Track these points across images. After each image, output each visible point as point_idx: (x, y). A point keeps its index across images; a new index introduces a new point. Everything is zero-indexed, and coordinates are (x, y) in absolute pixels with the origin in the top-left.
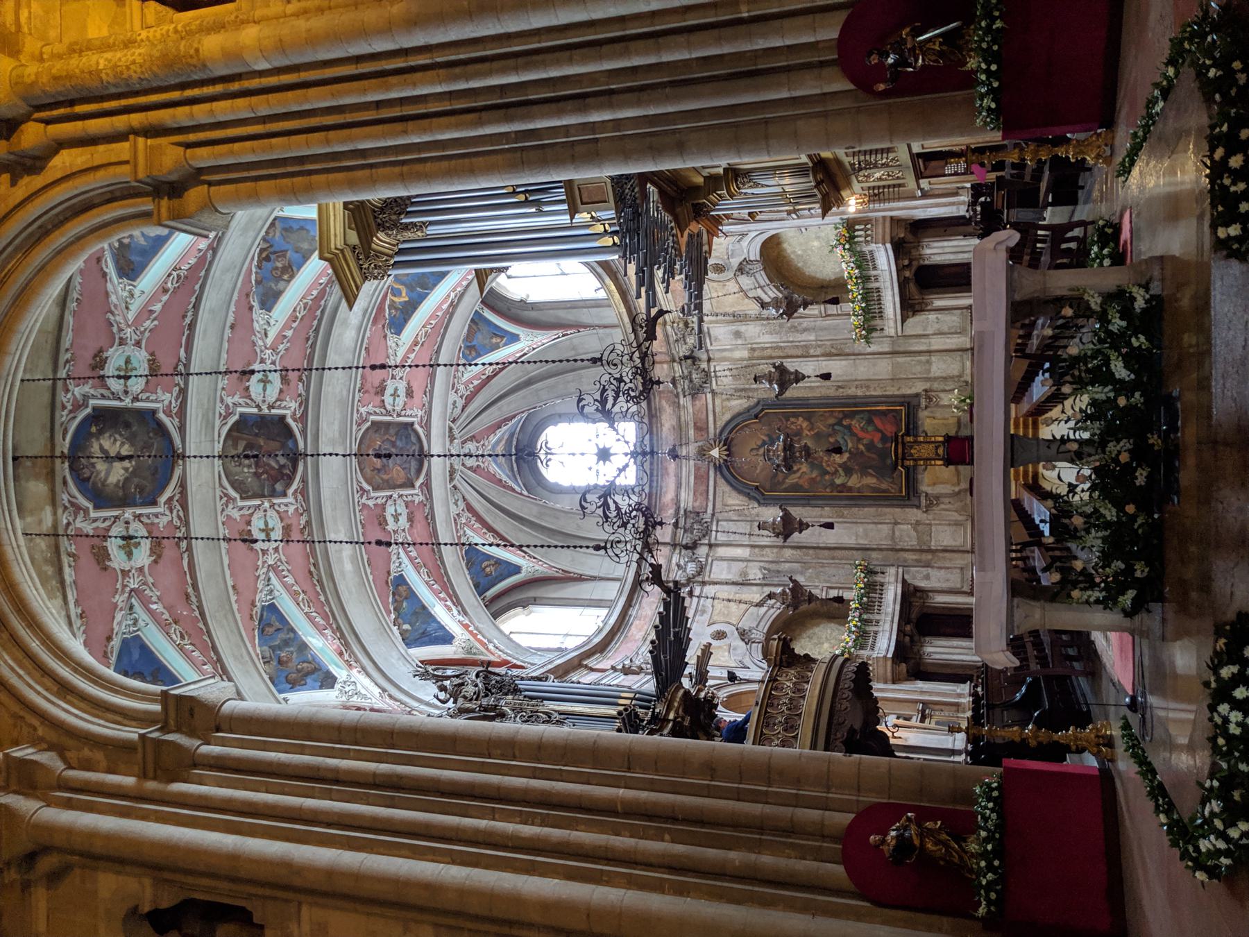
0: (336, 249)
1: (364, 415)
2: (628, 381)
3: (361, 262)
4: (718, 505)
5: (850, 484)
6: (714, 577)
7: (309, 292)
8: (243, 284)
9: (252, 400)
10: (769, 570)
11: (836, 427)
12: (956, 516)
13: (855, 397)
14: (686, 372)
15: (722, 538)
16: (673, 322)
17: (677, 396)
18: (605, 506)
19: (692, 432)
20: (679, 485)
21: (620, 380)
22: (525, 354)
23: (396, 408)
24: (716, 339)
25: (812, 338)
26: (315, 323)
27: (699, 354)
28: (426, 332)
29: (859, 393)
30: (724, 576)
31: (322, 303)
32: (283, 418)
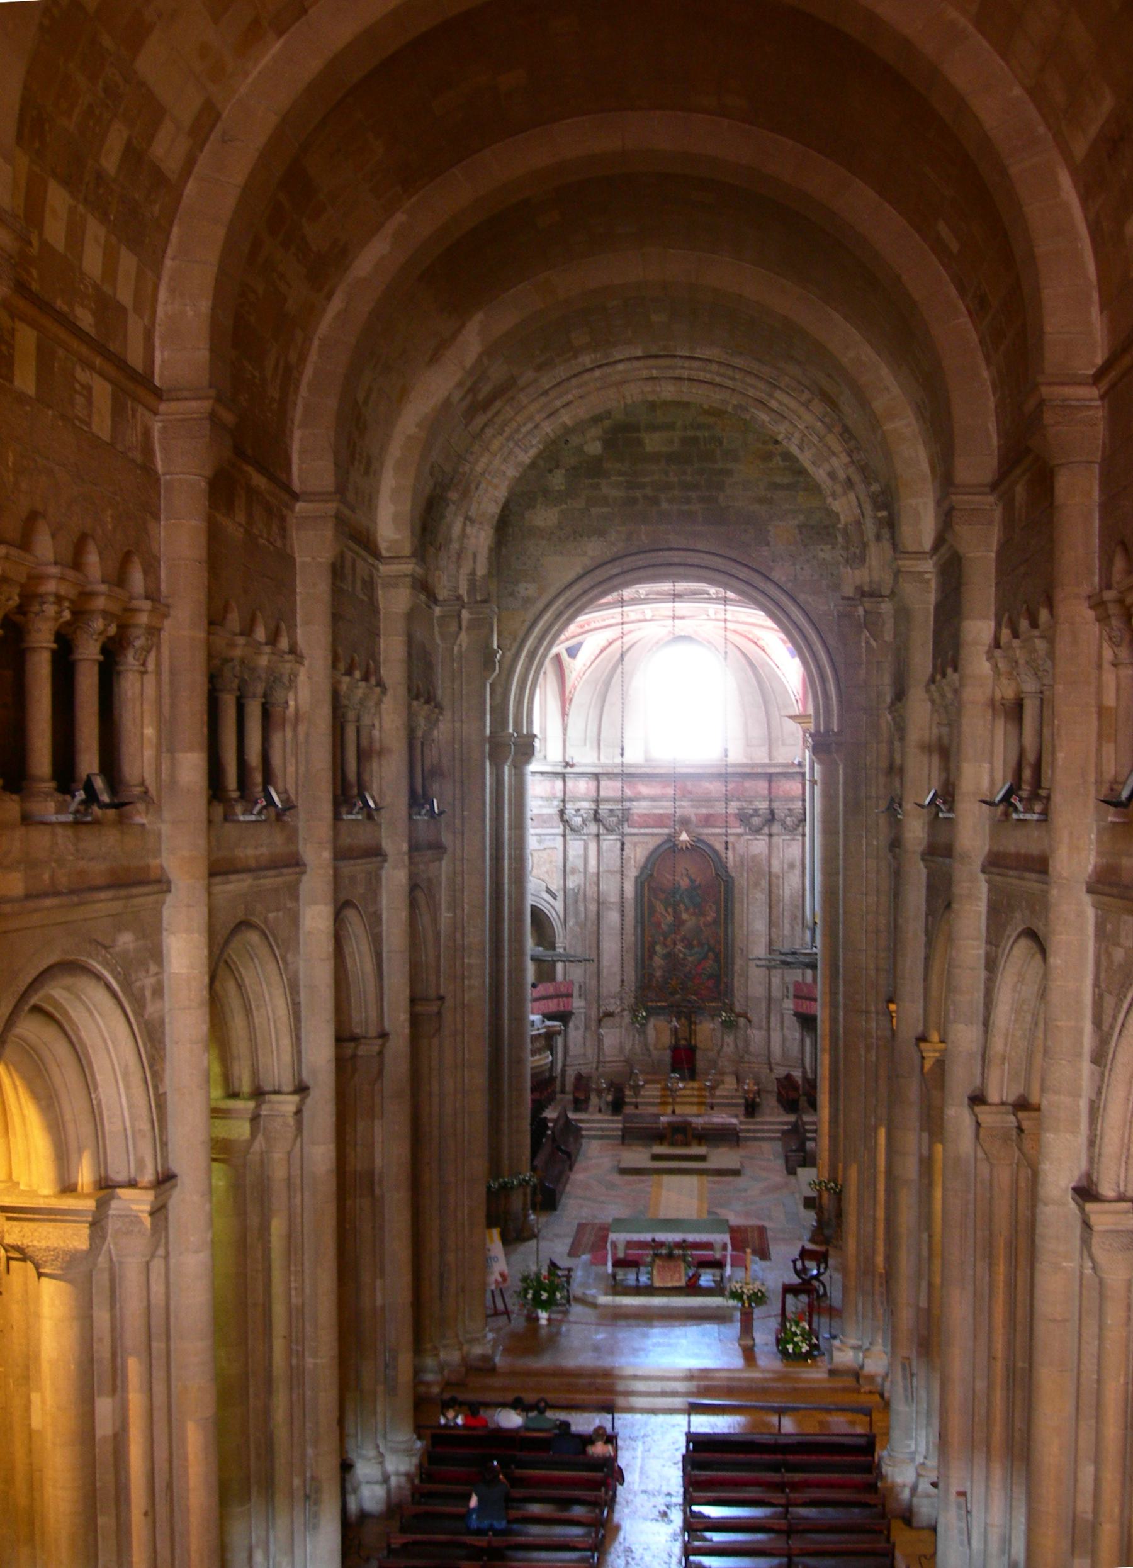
4: (635, 839)
5: (656, 958)
6: (570, 843)
10: (578, 893)
11: (706, 947)
12: (628, 1047)
13: (733, 964)
14: (761, 812)
15: (605, 845)
17: (738, 800)
19: (704, 811)
20: (653, 799)
24: (789, 846)
25: (787, 932)
27: (776, 828)
29: (737, 968)
30: (571, 853)
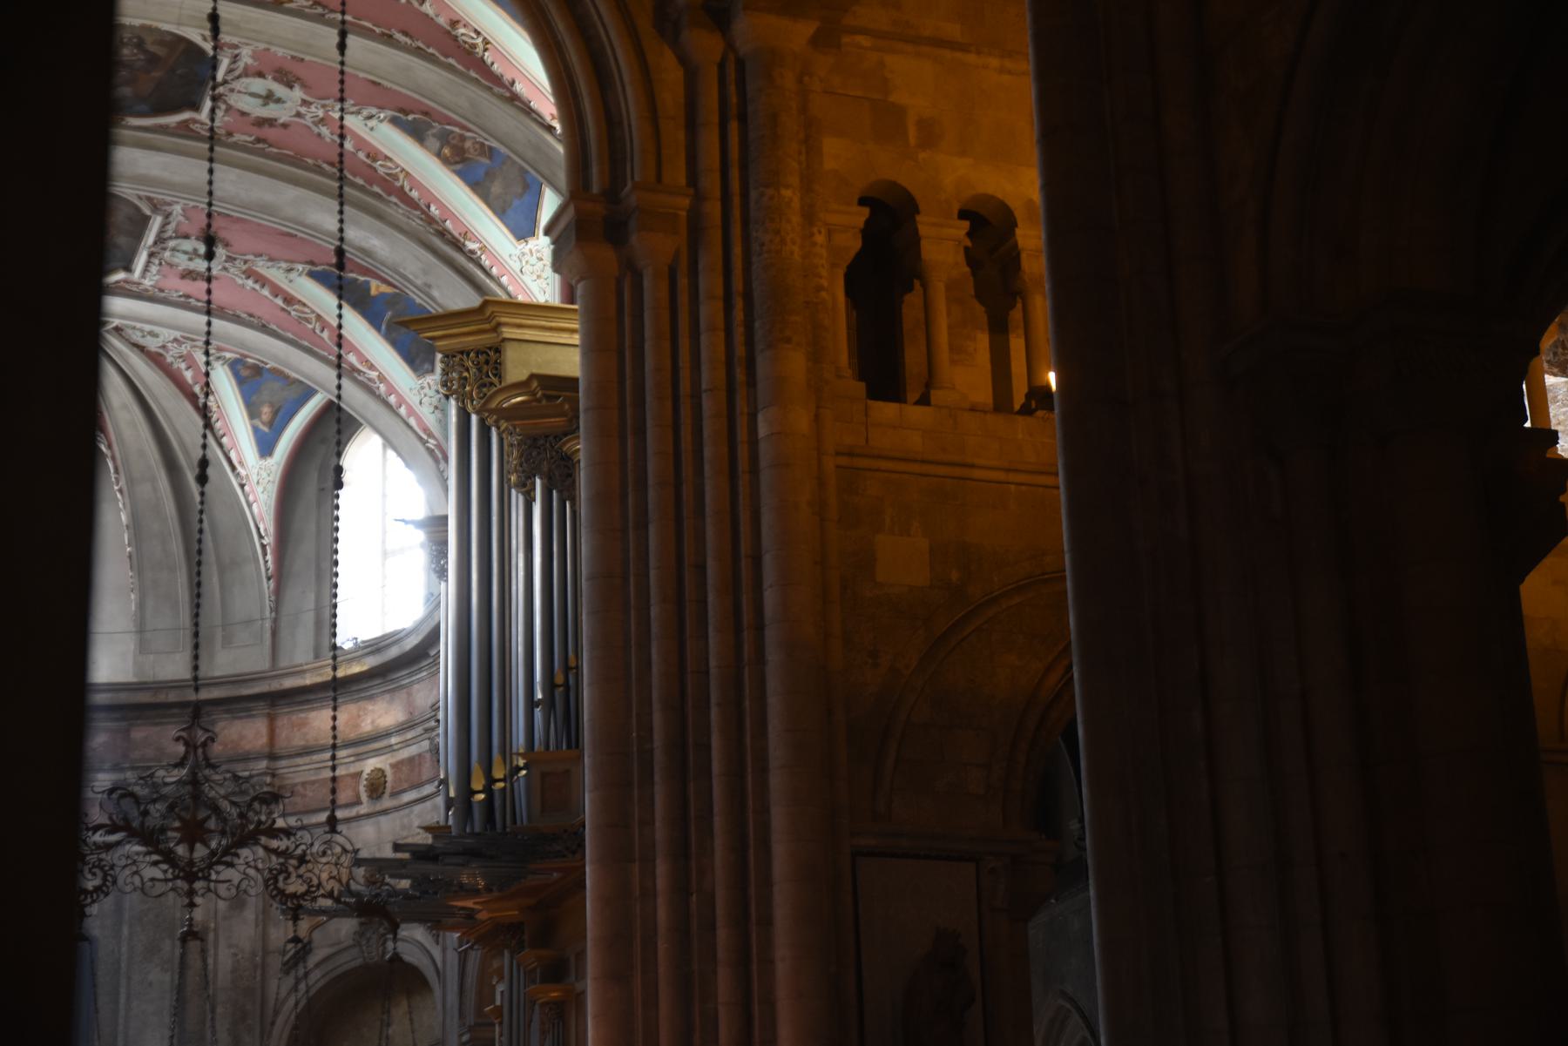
0: (499, 324)
1: (167, 208)
2: (302, 870)
3: (472, 355)
7: (416, 184)
8: (450, 118)
9: (239, 77)
14: (165, 790)
16: (273, 776)
18: (113, 829)
21: (302, 860)
22: (233, 468)
23: (167, 254)
26: (360, 181)
28: (308, 320)
31: (394, 199)
32: (196, 107)
